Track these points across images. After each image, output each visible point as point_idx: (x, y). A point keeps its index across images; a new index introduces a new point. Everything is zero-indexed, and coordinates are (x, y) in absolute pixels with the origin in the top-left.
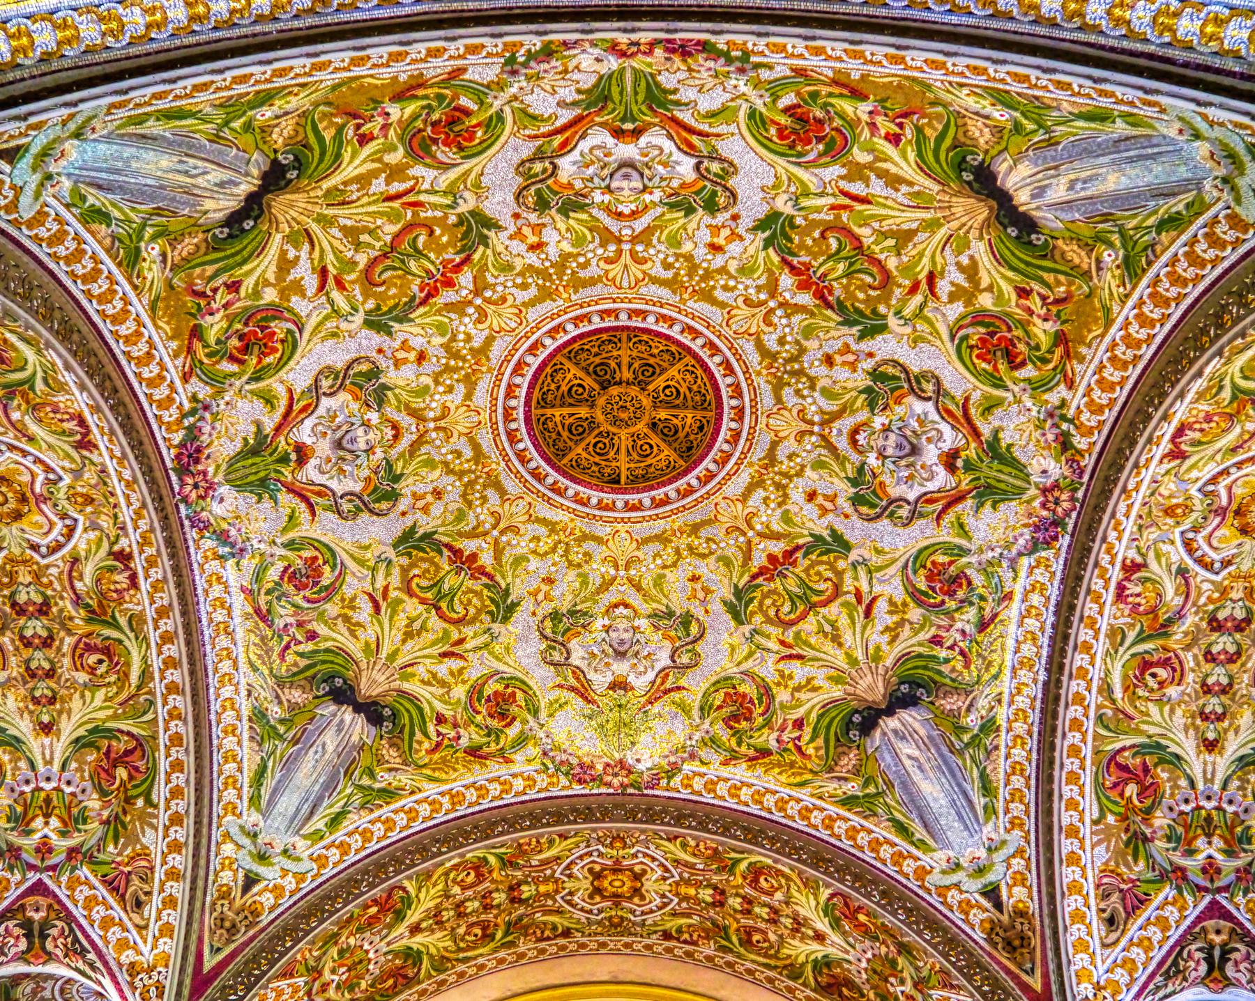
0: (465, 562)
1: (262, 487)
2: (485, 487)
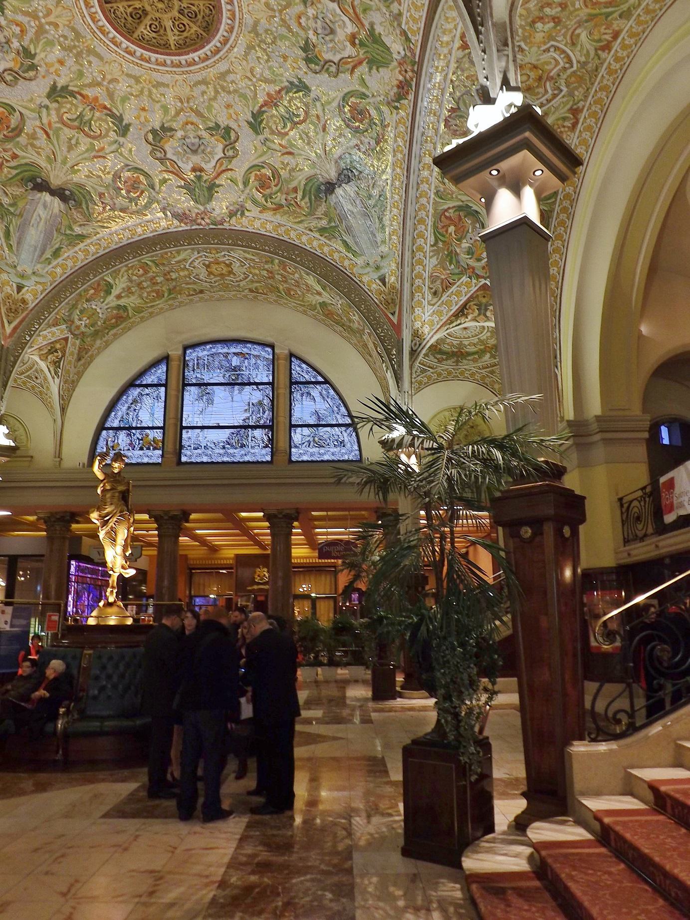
0: (272, 101)
1: (212, 188)
2: (225, 81)
